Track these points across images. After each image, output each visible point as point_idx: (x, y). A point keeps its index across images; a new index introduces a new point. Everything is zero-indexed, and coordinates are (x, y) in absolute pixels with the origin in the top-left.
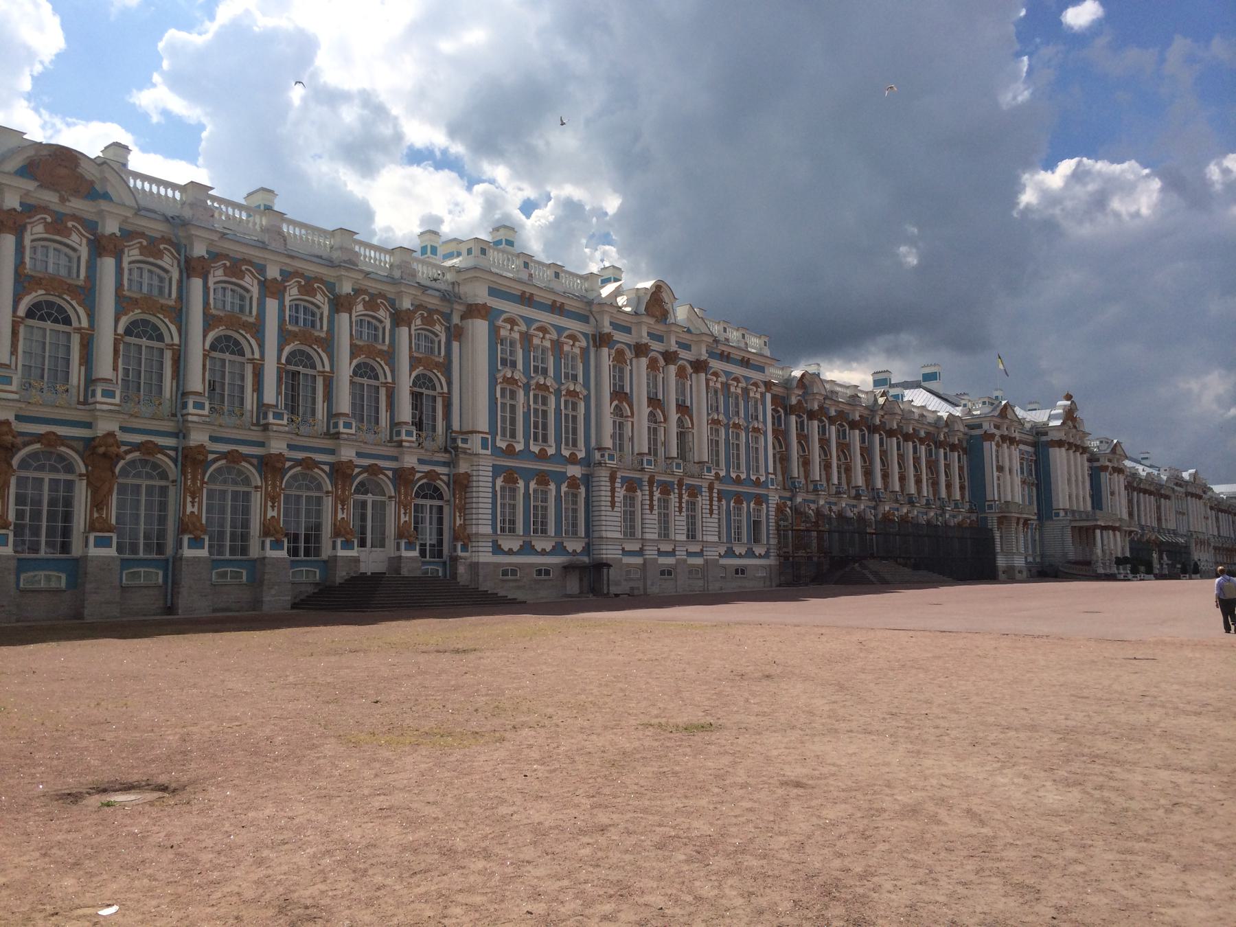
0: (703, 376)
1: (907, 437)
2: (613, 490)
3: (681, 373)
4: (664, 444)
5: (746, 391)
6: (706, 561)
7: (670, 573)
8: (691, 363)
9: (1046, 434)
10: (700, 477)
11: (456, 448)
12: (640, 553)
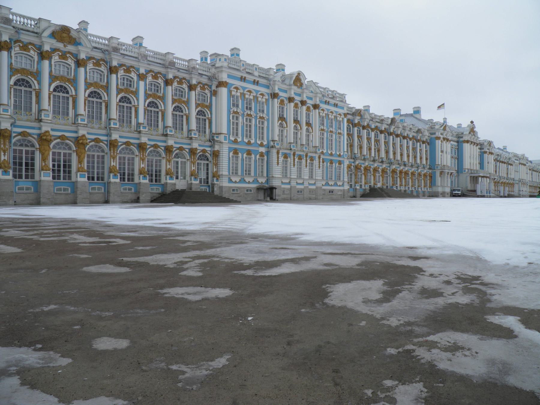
0: (317, 111)
1: (404, 138)
2: (278, 158)
3: (308, 109)
4: (300, 139)
5: (336, 117)
6: (317, 188)
8: (312, 105)
9: (462, 137)
10: (316, 153)
11: (214, 140)
12: (289, 183)
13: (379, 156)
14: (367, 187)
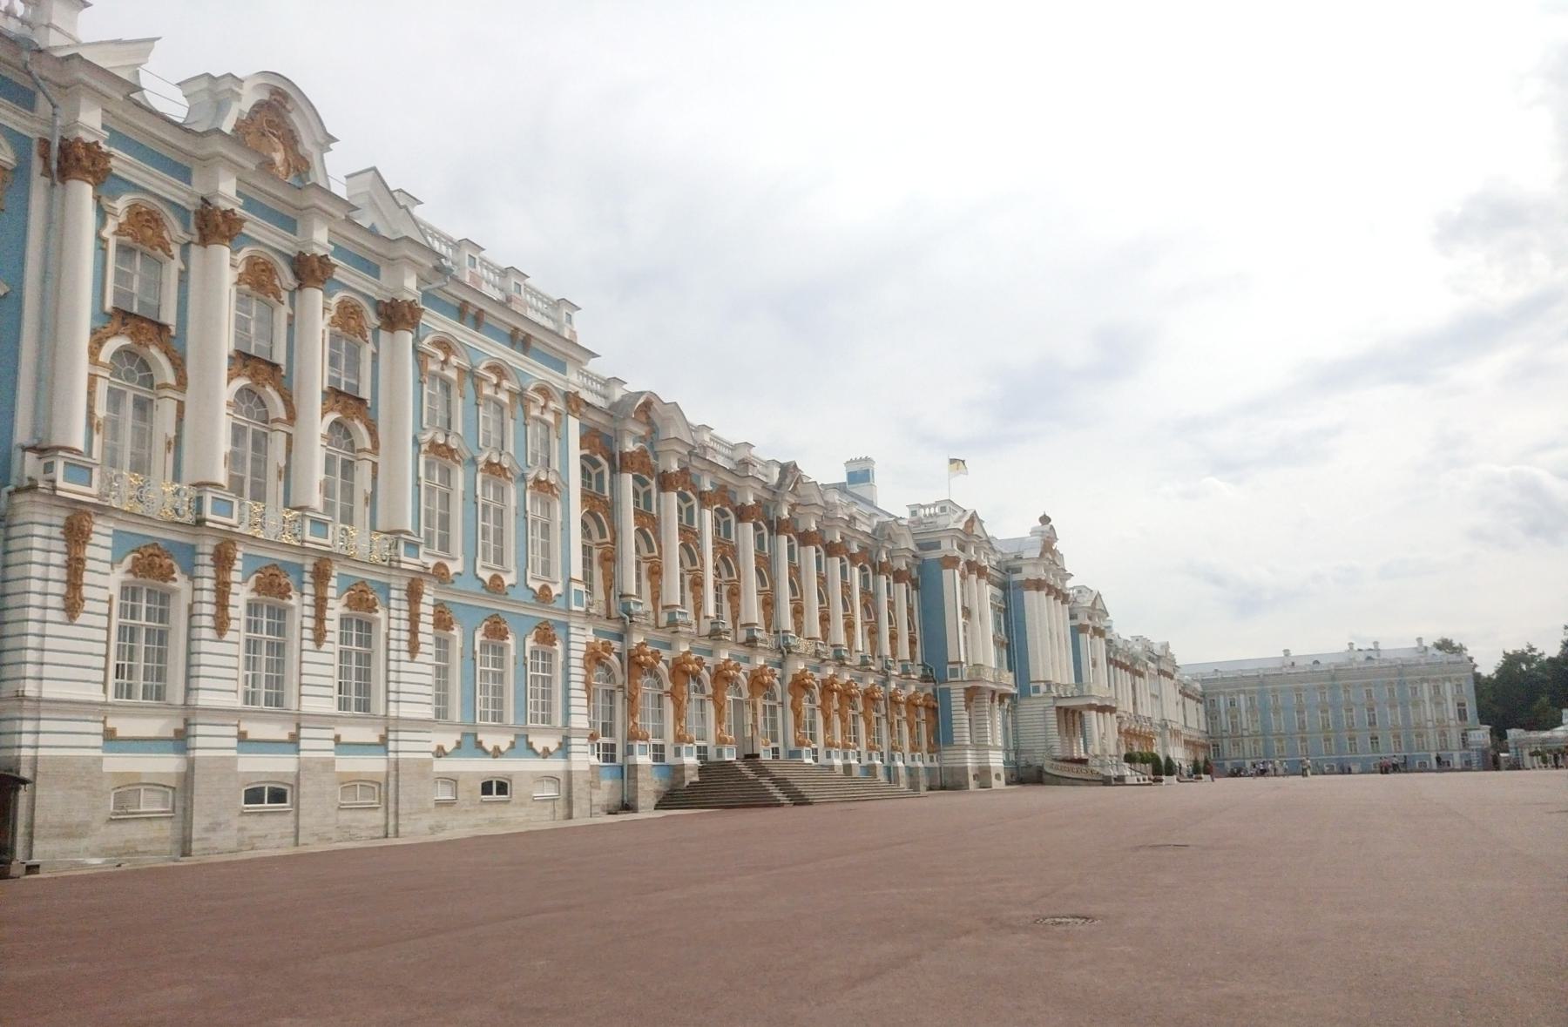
4: (286, 473)
7: (278, 796)
13: (735, 617)
14: (691, 761)
